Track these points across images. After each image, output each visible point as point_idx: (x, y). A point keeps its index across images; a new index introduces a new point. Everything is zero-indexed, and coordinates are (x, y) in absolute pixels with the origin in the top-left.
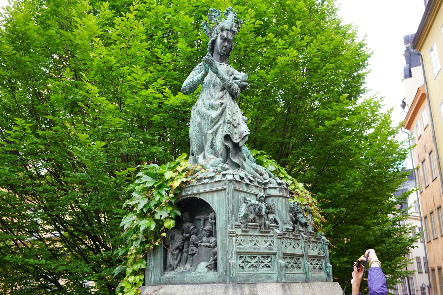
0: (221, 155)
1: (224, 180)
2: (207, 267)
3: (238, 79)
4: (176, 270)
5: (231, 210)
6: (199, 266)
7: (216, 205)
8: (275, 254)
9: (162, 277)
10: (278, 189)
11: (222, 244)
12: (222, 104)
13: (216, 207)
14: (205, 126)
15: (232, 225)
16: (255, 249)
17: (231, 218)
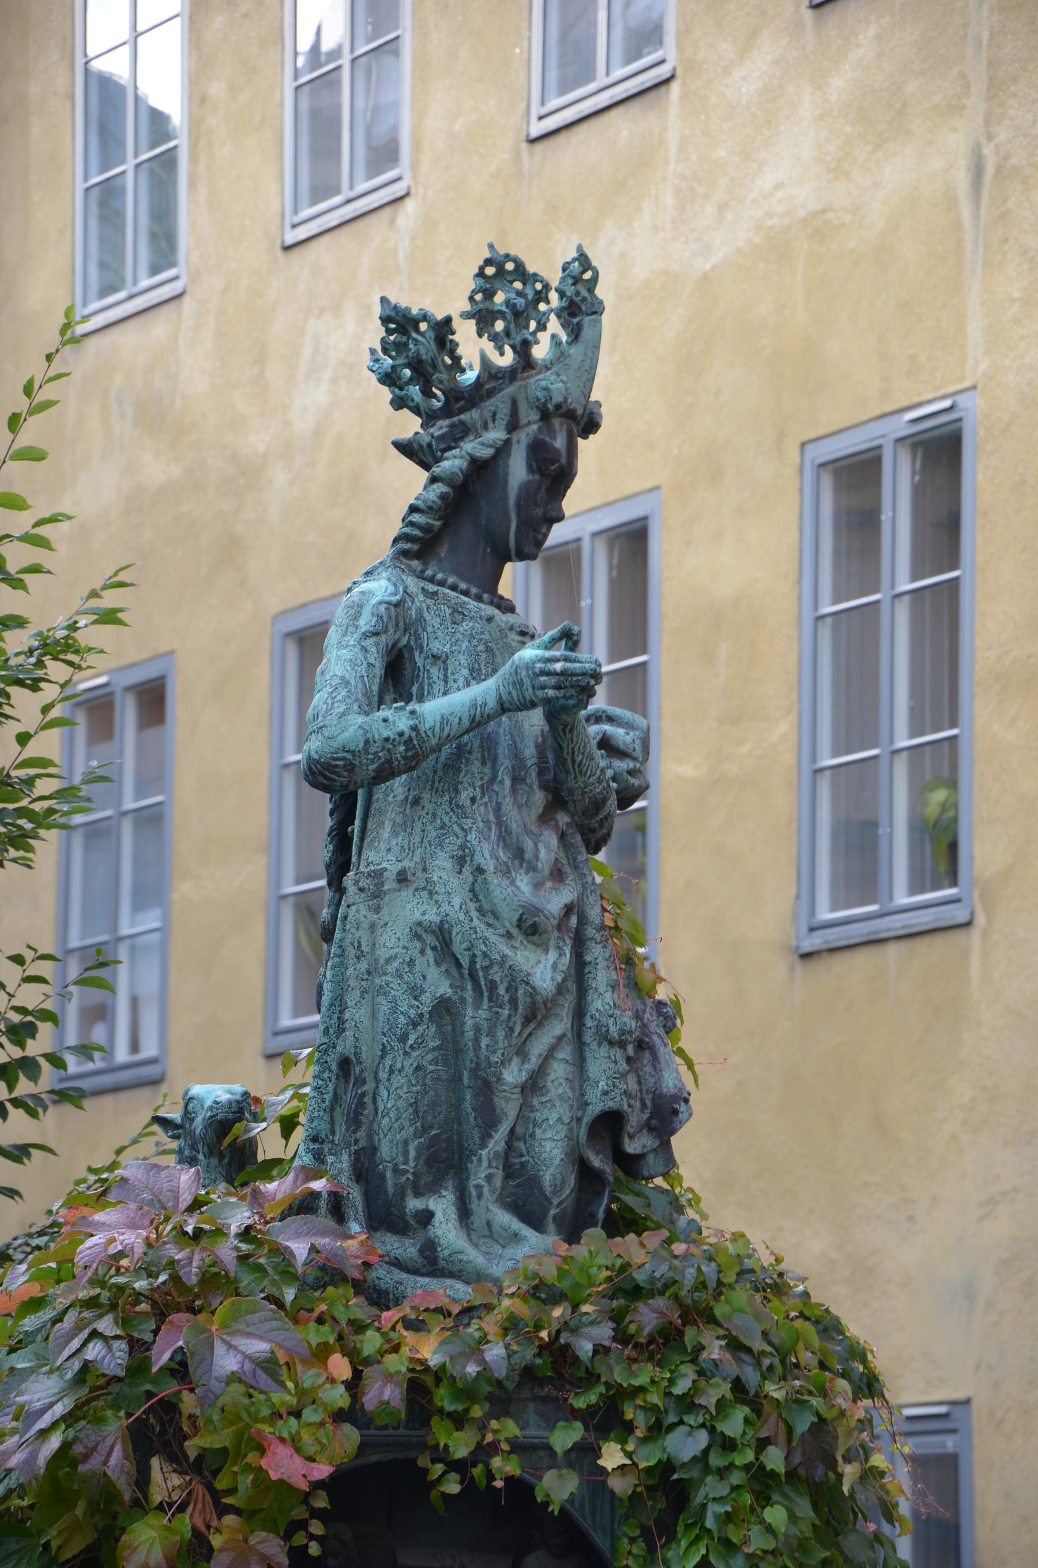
14: (491, 1034)
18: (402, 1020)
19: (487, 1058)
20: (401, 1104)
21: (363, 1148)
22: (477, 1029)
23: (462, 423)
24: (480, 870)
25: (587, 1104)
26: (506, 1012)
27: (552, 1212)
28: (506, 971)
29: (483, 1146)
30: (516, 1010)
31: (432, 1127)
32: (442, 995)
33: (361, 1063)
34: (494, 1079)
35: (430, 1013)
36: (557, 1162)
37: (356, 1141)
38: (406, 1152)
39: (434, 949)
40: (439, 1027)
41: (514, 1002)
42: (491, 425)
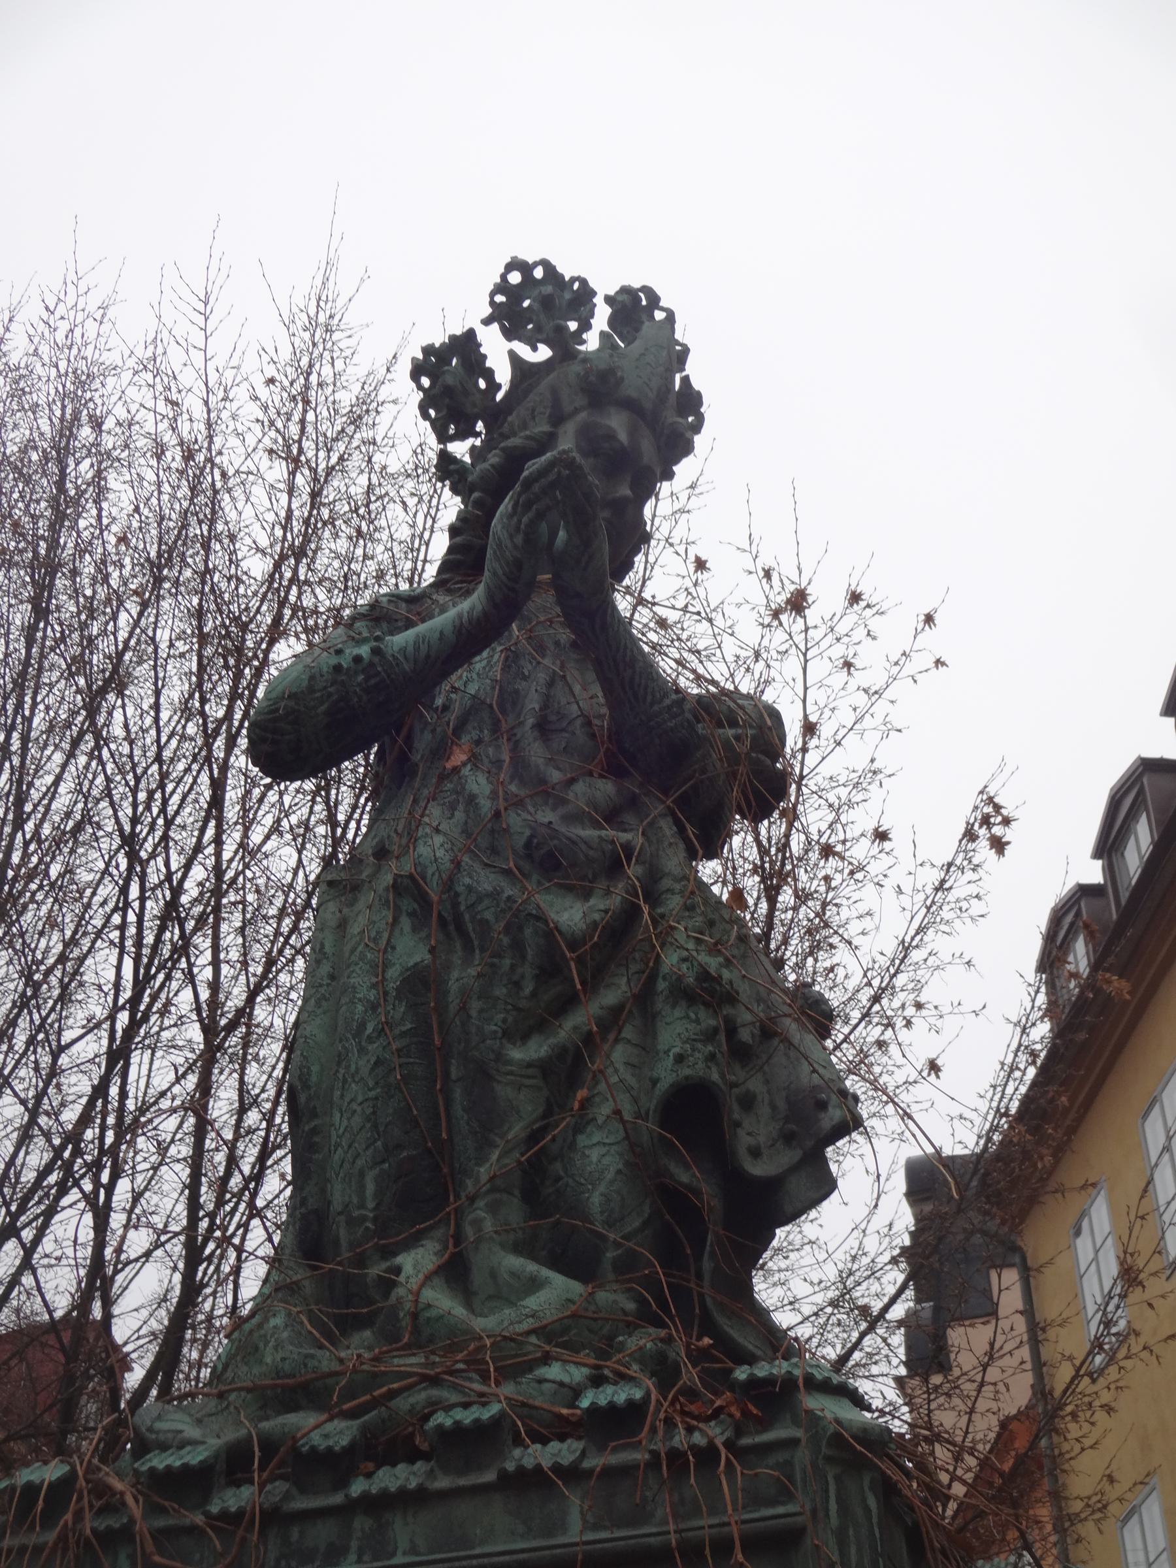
12: (614, 866)
18: (360, 1008)
20: (357, 1121)
26: (507, 962)
27: (609, 1255)
28: (502, 905)
30: (523, 957)
32: (416, 964)
33: (309, 1088)
34: (492, 1056)
35: (397, 989)
36: (610, 1176)
38: (362, 1187)
41: (518, 947)
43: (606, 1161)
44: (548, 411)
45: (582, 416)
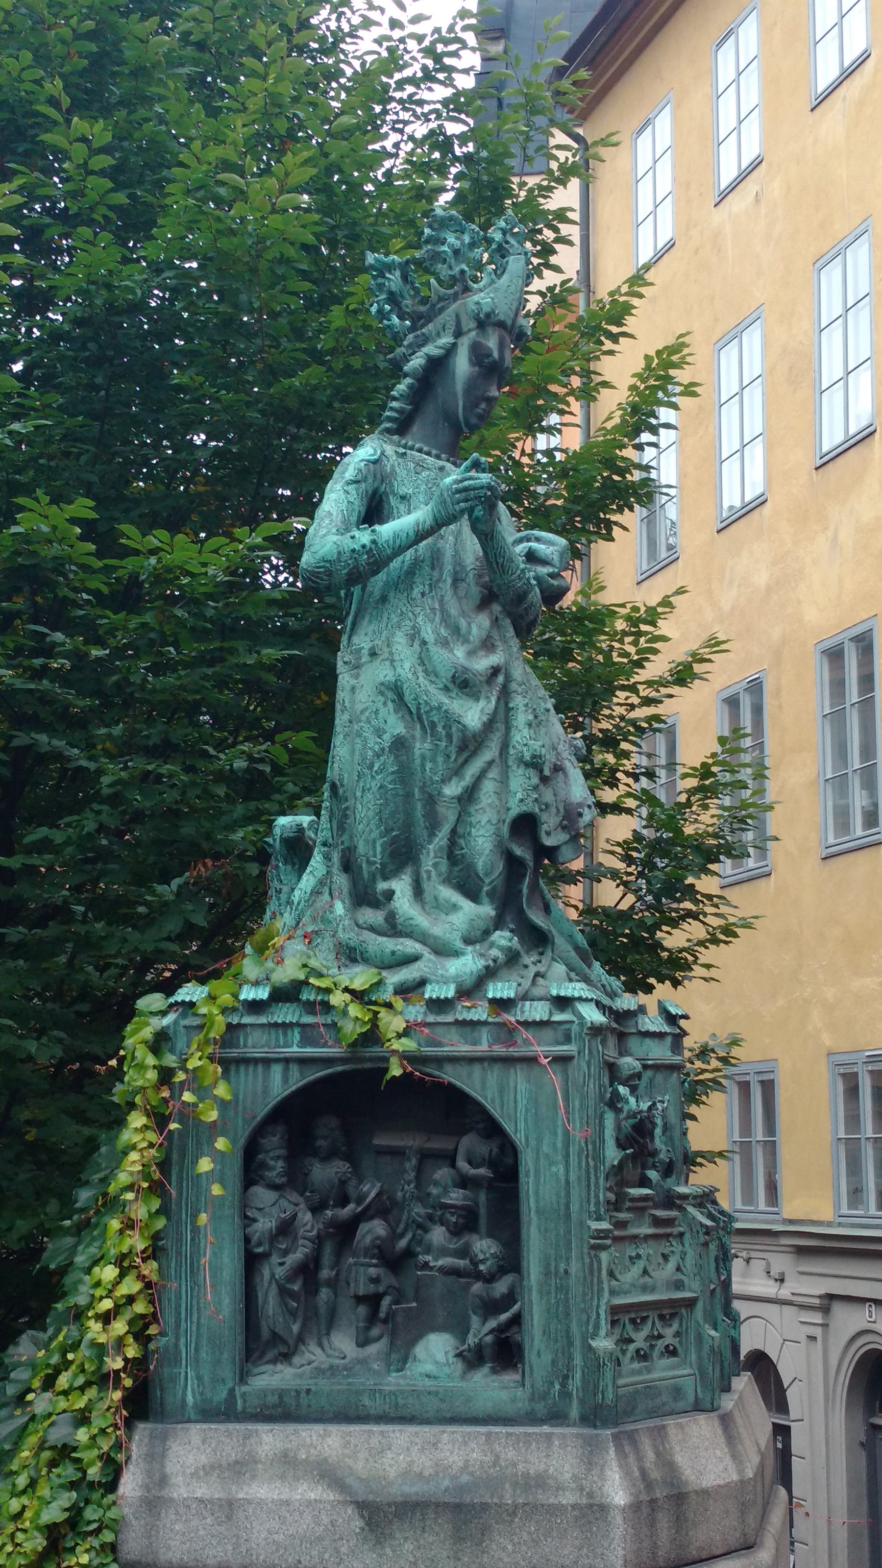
0: (491, 895)
1: (560, 1023)
2: (459, 1355)
3: (544, 562)
4: (296, 1360)
5: (594, 1143)
6: (419, 1350)
7: (521, 1116)
8: (690, 1303)
9: (244, 1388)
10: (669, 1039)
11: (547, 1273)
13: (521, 1125)
14: (433, 760)
15: (597, 1203)
16: (644, 1289)
17: (597, 1178)
18: (370, 753)
19: (431, 778)
20: (371, 813)
21: (348, 848)
22: (423, 757)
23: (423, 334)
24: (424, 643)
25: (509, 809)
26: (444, 744)
27: (485, 889)
29: (430, 842)
31: (392, 830)
36: (487, 852)
37: (342, 843)
38: (374, 848)
39: (393, 701)
40: (396, 757)
41: (449, 736)
42: (442, 334)
43: (486, 845)
44: (453, 328)
45: (474, 333)
